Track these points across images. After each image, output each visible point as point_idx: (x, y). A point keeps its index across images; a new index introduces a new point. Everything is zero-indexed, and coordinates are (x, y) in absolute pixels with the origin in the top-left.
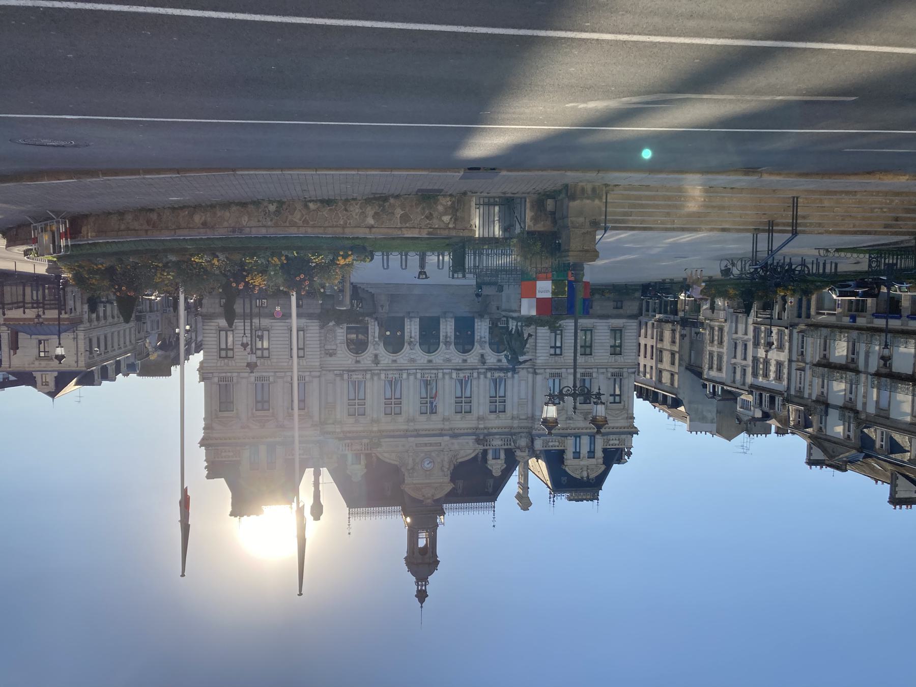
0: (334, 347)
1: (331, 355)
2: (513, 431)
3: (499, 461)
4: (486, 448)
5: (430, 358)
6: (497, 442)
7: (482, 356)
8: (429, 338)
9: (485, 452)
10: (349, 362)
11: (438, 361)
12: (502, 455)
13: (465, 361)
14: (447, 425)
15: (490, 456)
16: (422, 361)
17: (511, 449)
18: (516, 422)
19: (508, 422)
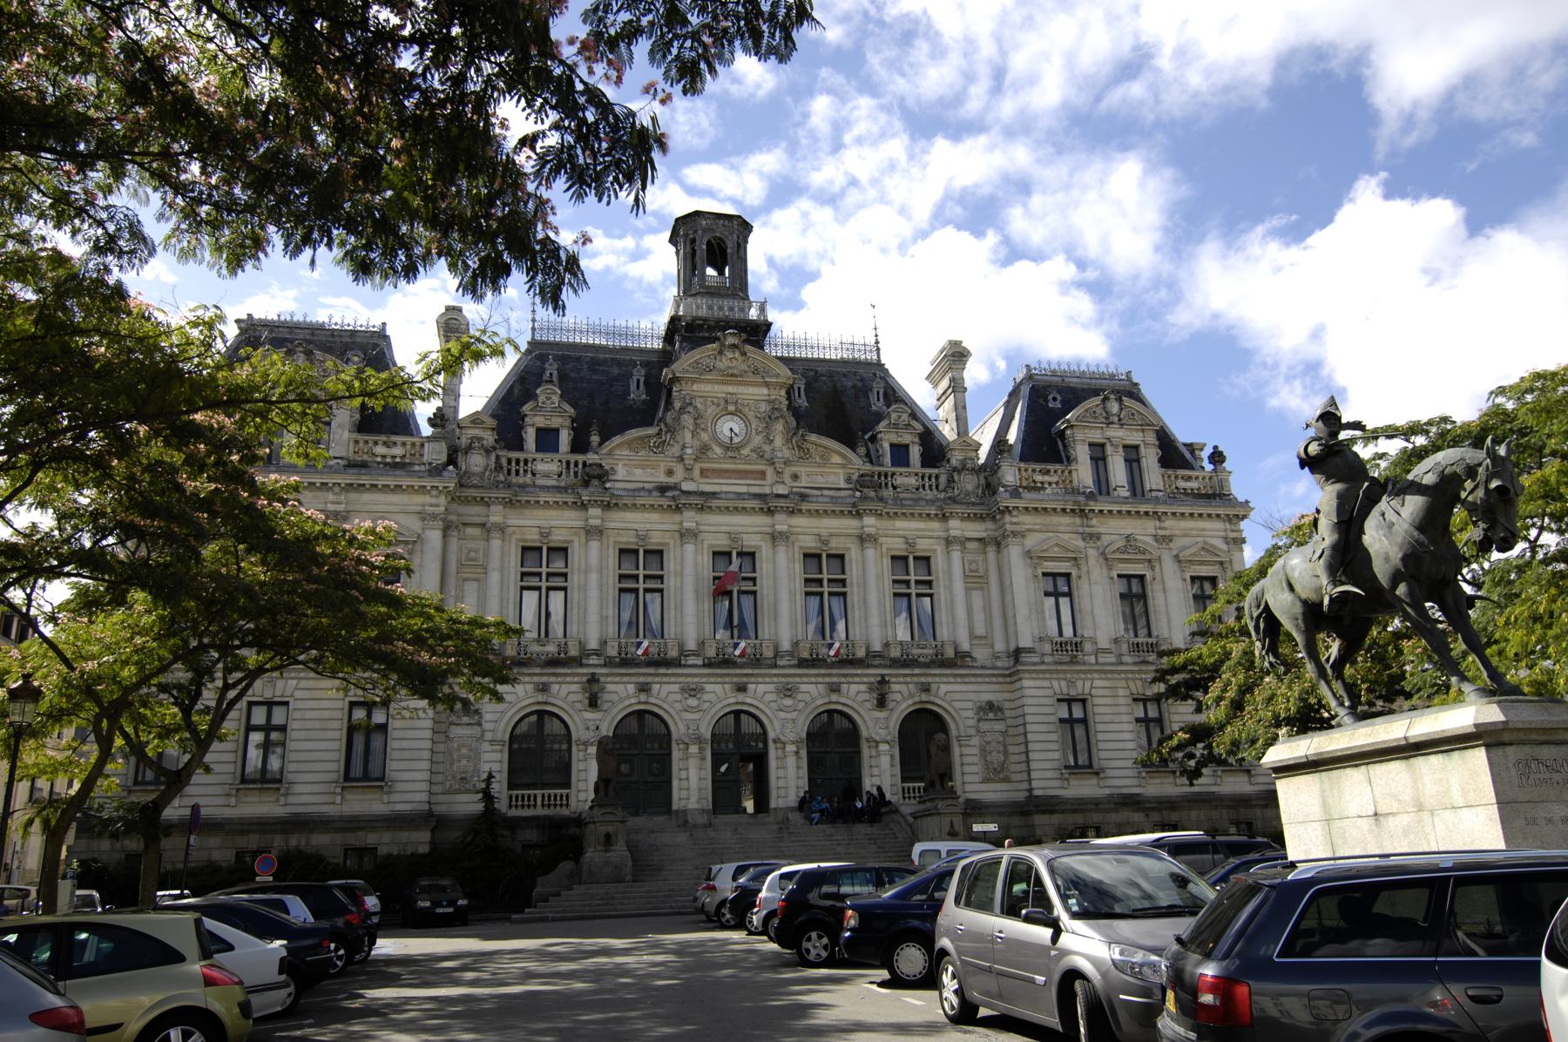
0: (984, 726)
1: (991, 706)
2: (506, 494)
3: (540, 421)
4: (580, 458)
5: (740, 697)
6: (547, 466)
7: (593, 703)
8: (740, 753)
9: (579, 445)
10: (944, 688)
11: (718, 688)
12: (530, 436)
13: (644, 688)
14: (690, 519)
15: (565, 438)
16: (761, 688)
17: (510, 447)
18: (494, 519)
19: (515, 519)
